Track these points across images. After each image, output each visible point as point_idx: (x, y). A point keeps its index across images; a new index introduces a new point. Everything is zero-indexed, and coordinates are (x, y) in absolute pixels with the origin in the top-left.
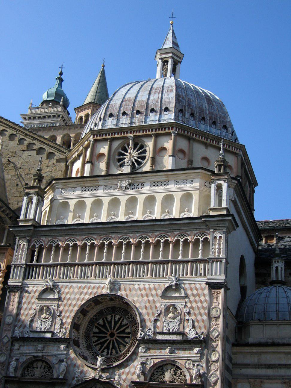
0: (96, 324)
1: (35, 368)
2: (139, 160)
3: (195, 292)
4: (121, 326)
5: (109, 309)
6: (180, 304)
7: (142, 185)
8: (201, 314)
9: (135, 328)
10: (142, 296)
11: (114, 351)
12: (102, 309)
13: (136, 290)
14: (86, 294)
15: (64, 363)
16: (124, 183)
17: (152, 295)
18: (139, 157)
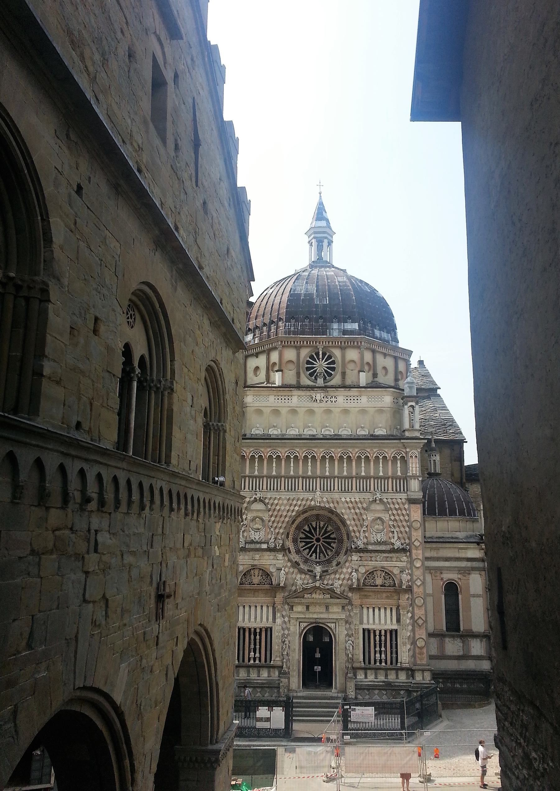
0: (302, 531)
1: (253, 576)
2: (328, 370)
3: (397, 506)
4: (326, 532)
6: (386, 517)
7: (335, 397)
8: (404, 527)
10: (349, 508)
11: (321, 555)
14: (295, 505)
15: (282, 571)
16: (319, 396)
17: (359, 508)
18: (327, 368)
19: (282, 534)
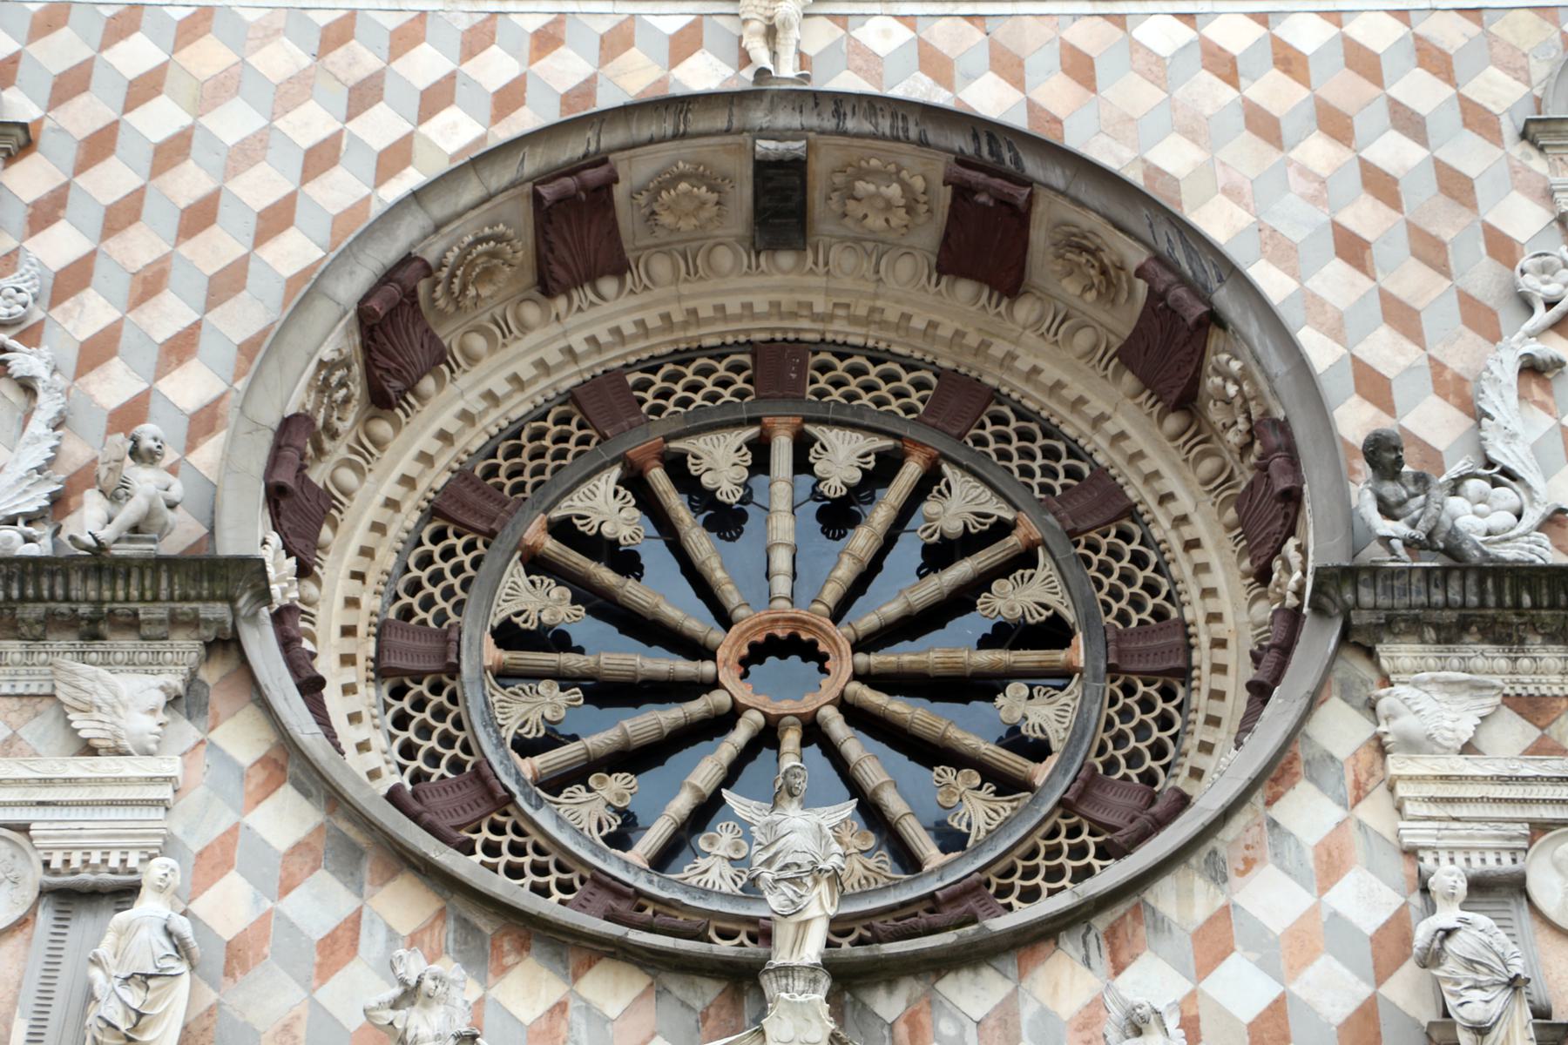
0: (535, 533)
5: (706, 372)
9: (1127, 578)
10: (1264, 125)
12: (613, 358)
13: (1157, 69)
14: (435, 99)
17: (1409, 123)
19: (204, 422)
